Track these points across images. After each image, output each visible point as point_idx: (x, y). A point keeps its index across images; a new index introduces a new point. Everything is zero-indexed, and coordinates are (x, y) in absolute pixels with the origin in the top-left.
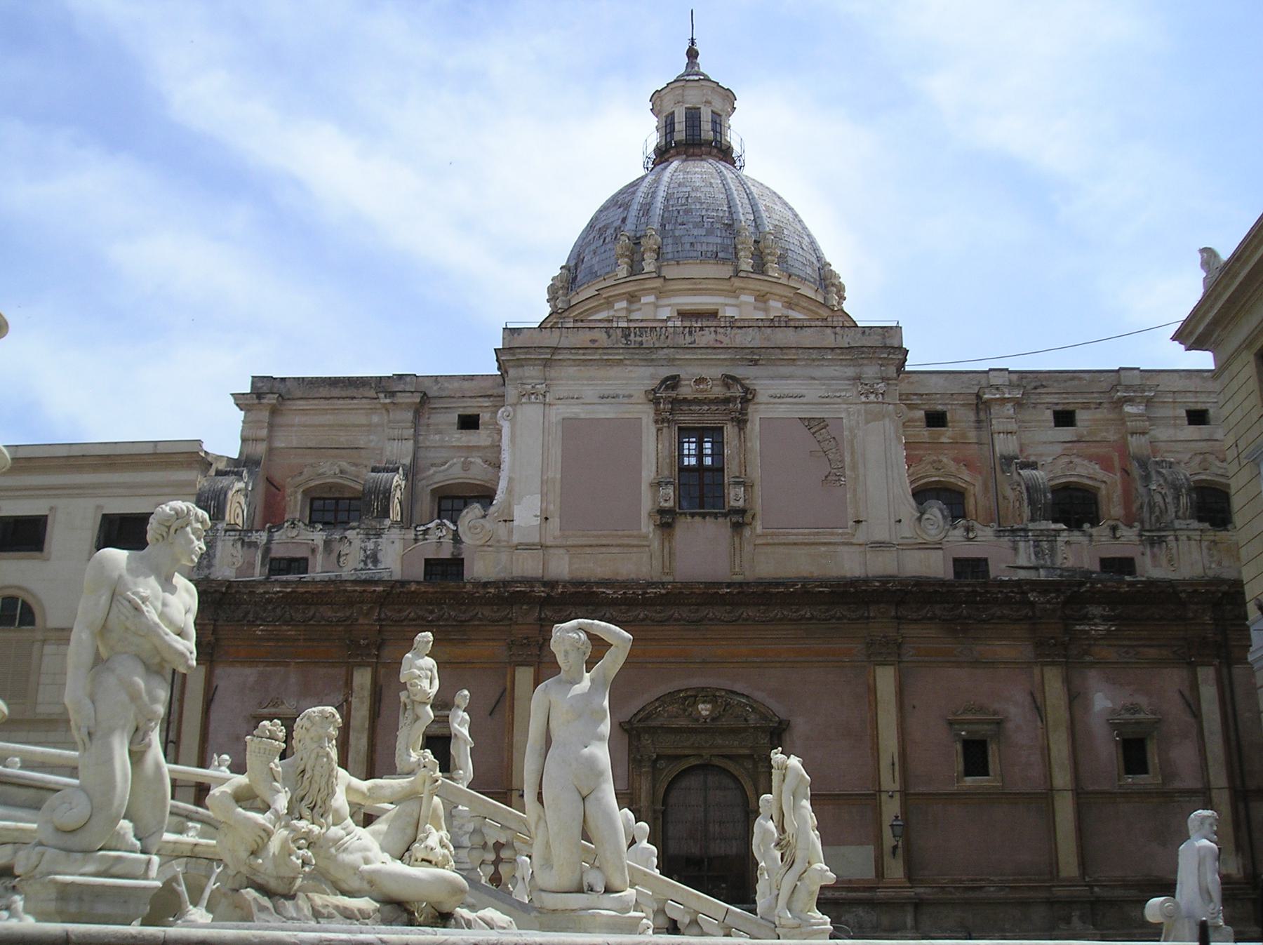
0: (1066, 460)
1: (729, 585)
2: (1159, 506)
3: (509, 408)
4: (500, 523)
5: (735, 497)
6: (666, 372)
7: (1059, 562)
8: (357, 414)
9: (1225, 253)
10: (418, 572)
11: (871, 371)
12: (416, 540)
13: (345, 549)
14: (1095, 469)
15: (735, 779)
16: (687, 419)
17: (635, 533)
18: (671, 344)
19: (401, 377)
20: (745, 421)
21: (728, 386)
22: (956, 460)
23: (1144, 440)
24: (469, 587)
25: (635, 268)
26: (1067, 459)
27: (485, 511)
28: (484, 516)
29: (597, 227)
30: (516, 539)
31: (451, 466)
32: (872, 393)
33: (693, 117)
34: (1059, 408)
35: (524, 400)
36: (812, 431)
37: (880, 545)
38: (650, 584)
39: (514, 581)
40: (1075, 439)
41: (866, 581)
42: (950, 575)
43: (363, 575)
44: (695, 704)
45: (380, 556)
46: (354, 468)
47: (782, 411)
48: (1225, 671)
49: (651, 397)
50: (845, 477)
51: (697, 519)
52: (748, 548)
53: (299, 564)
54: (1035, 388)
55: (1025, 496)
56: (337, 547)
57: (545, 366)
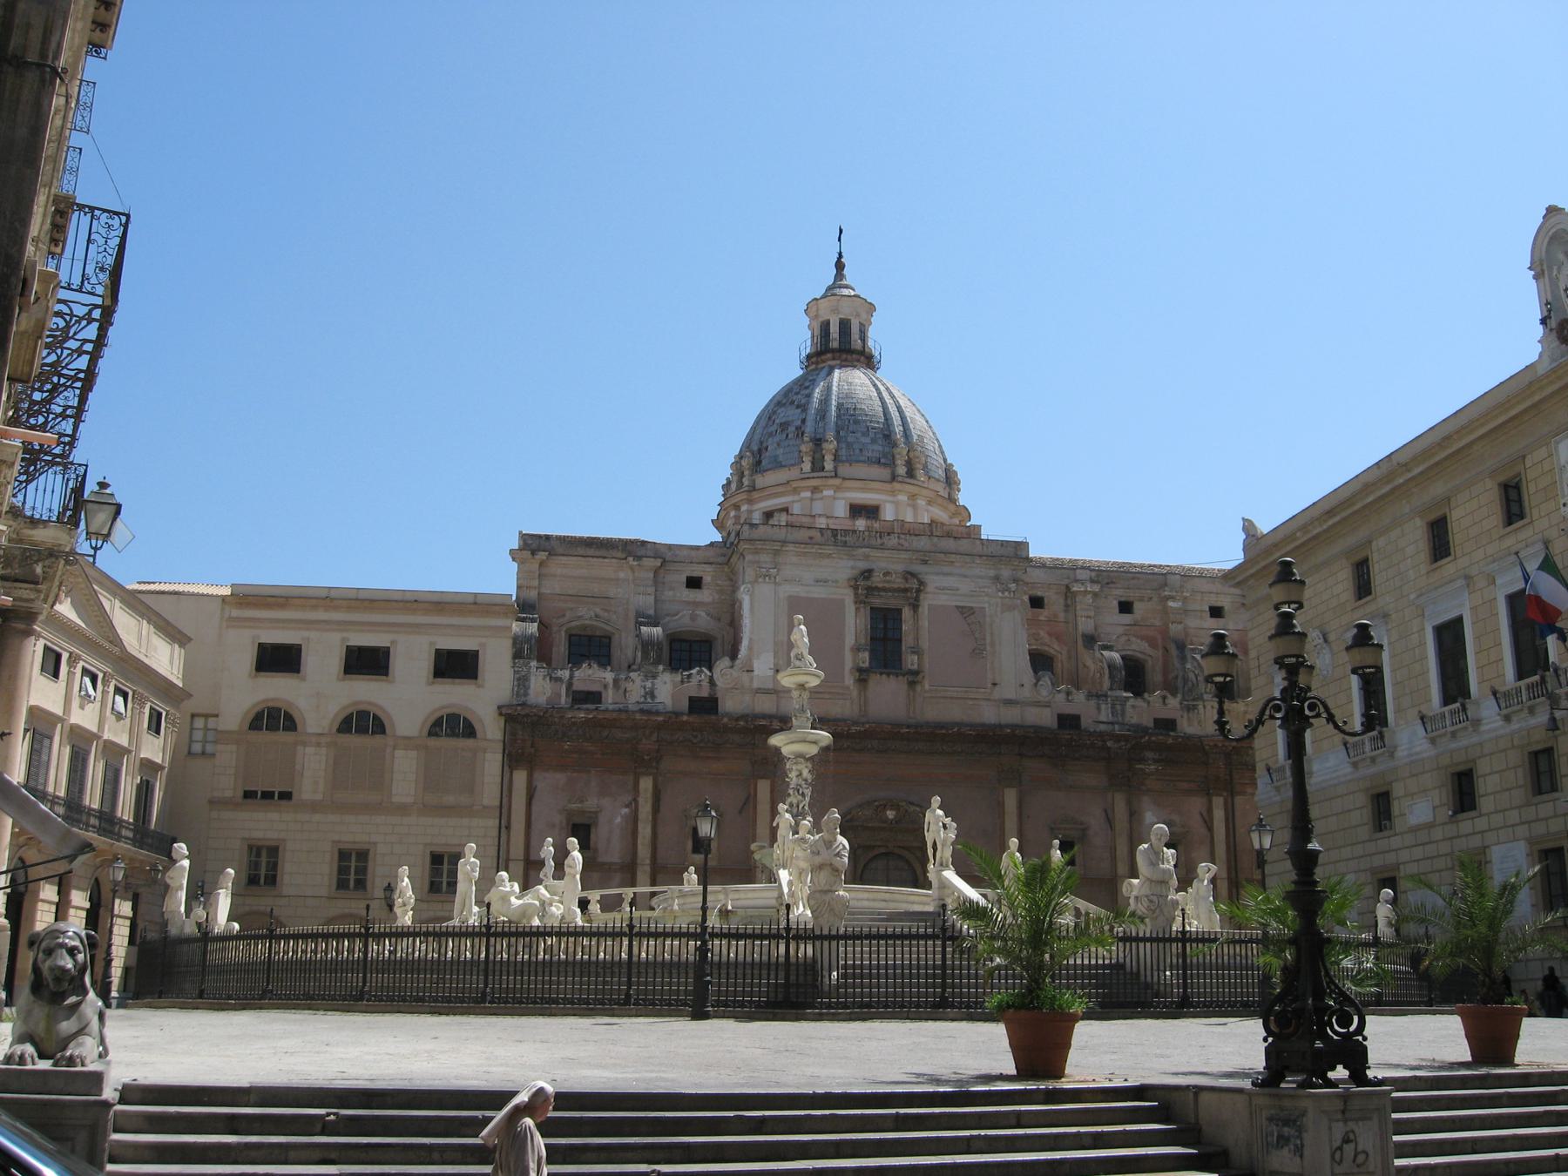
1: (908, 727)
3: (749, 586)
5: (911, 661)
6: (863, 565)
7: (1127, 720)
8: (606, 568)
9: (1265, 526)
10: (685, 705)
11: (1006, 573)
12: (682, 682)
13: (629, 686)
14: (1149, 650)
15: (907, 862)
16: (877, 602)
19: (644, 543)
20: (918, 606)
21: (906, 579)
22: (1050, 634)
23: (1180, 627)
24: (725, 720)
25: (818, 466)
26: (1126, 638)
28: (732, 667)
29: (777, 421)
30: (756, 685)
31: (681, 617)
33: (845, 325)
34: (1123, 599)
35: (760, 580)
37: (1009, 702)
38: (855, 723)
39: (756, 717)
41: (1000, 726)
42: (1055, 726)
43: (645, 707)
44: (885, 807)
45: (656, 693)
46: (606, 614)
47: (943, 600)
48: (1230, 800)
49: (852, 584)
51: (884, 676)
53: (593, 697)
54: (1108, 583)
55: (1107, 671)
56: (623, 685)
57: (775, 555)
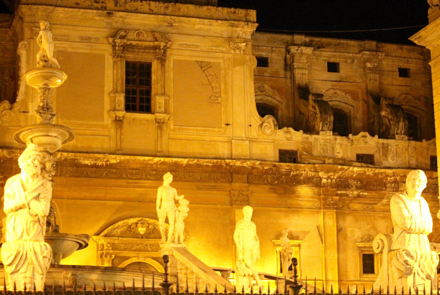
0: (332, 91)
2: (386, 125)
4: (20, 113)
16: (132, 57)
17: (101, 123)
18: (123, 8)
20: (165, 60)
22: (273, 88)
27: (11, 105)
28: (11, 109)
32: (238, 49)
36: (203, 69)
40: (338, 80)
50: (221, 98)
52: (165, 137)
